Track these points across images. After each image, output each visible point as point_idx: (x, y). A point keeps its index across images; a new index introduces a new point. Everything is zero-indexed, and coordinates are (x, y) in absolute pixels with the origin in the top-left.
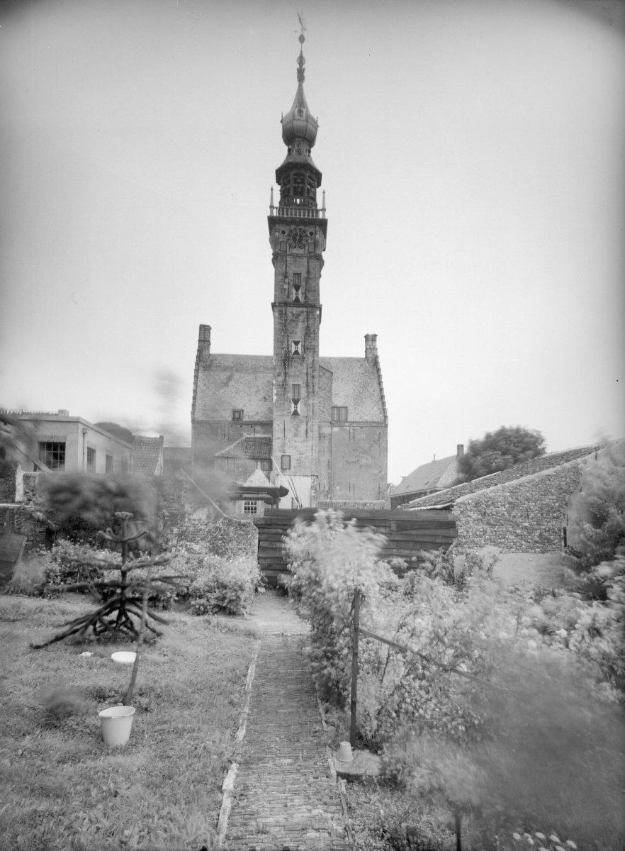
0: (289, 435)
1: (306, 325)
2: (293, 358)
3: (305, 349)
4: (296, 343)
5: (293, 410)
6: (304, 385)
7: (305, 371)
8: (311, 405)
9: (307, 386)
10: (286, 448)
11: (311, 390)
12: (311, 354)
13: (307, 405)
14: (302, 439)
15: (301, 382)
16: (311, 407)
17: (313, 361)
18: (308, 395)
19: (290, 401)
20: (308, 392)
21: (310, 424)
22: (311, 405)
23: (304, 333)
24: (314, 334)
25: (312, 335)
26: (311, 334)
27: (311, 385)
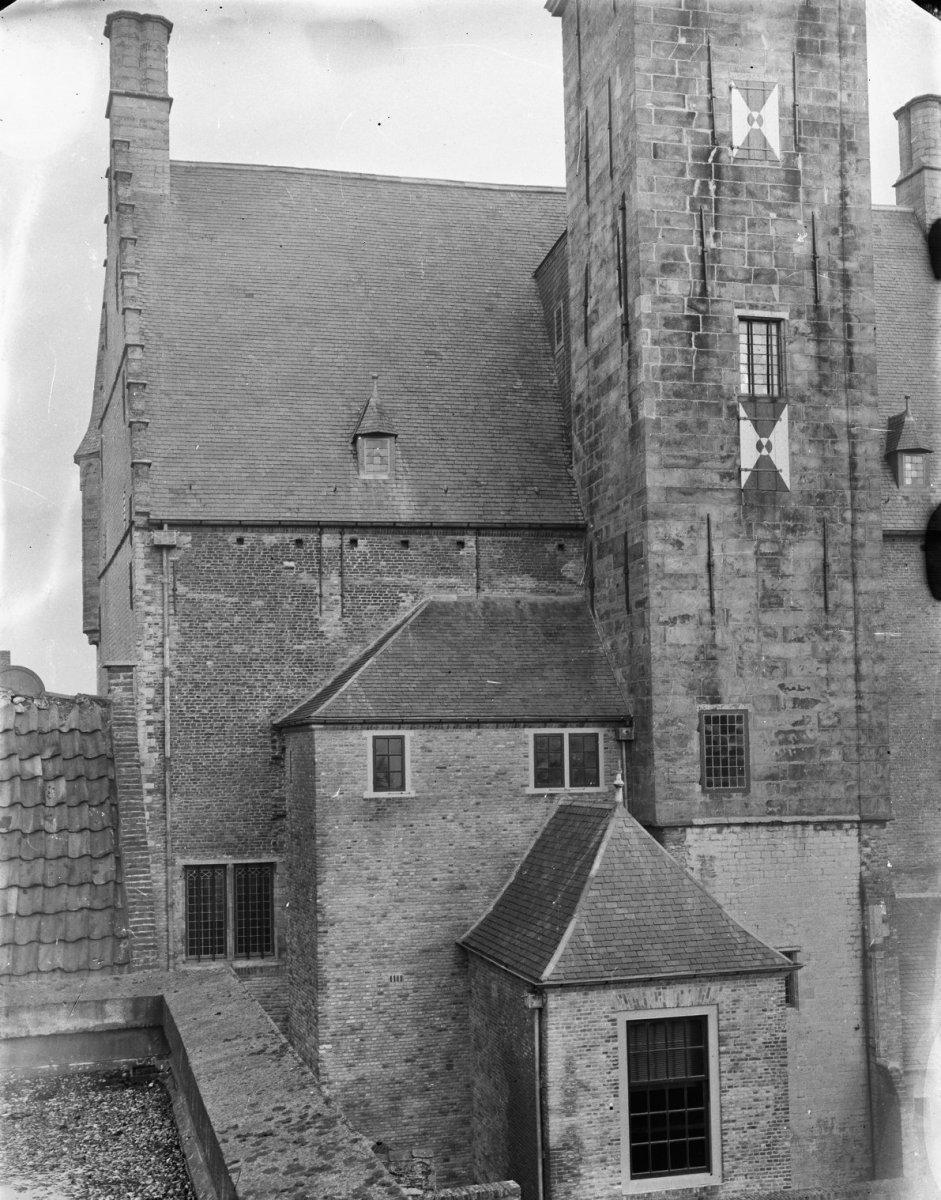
5: (748, 458)
6: (802, 324)
8: (842, 433)
9: (820, 330)
10: (724, 673)
11: (839, 349)
12: (830, 158)
13: (821, 434)
14: (804, 618)
16: (843, 447)
17: (844, 194)
19: (733, 412)
20: (821, 359)
21: (842, 533)
22: (842, 433)
24: (842, 50)
25: (832, 57)
26: (824, 48)
27: (835, 325)
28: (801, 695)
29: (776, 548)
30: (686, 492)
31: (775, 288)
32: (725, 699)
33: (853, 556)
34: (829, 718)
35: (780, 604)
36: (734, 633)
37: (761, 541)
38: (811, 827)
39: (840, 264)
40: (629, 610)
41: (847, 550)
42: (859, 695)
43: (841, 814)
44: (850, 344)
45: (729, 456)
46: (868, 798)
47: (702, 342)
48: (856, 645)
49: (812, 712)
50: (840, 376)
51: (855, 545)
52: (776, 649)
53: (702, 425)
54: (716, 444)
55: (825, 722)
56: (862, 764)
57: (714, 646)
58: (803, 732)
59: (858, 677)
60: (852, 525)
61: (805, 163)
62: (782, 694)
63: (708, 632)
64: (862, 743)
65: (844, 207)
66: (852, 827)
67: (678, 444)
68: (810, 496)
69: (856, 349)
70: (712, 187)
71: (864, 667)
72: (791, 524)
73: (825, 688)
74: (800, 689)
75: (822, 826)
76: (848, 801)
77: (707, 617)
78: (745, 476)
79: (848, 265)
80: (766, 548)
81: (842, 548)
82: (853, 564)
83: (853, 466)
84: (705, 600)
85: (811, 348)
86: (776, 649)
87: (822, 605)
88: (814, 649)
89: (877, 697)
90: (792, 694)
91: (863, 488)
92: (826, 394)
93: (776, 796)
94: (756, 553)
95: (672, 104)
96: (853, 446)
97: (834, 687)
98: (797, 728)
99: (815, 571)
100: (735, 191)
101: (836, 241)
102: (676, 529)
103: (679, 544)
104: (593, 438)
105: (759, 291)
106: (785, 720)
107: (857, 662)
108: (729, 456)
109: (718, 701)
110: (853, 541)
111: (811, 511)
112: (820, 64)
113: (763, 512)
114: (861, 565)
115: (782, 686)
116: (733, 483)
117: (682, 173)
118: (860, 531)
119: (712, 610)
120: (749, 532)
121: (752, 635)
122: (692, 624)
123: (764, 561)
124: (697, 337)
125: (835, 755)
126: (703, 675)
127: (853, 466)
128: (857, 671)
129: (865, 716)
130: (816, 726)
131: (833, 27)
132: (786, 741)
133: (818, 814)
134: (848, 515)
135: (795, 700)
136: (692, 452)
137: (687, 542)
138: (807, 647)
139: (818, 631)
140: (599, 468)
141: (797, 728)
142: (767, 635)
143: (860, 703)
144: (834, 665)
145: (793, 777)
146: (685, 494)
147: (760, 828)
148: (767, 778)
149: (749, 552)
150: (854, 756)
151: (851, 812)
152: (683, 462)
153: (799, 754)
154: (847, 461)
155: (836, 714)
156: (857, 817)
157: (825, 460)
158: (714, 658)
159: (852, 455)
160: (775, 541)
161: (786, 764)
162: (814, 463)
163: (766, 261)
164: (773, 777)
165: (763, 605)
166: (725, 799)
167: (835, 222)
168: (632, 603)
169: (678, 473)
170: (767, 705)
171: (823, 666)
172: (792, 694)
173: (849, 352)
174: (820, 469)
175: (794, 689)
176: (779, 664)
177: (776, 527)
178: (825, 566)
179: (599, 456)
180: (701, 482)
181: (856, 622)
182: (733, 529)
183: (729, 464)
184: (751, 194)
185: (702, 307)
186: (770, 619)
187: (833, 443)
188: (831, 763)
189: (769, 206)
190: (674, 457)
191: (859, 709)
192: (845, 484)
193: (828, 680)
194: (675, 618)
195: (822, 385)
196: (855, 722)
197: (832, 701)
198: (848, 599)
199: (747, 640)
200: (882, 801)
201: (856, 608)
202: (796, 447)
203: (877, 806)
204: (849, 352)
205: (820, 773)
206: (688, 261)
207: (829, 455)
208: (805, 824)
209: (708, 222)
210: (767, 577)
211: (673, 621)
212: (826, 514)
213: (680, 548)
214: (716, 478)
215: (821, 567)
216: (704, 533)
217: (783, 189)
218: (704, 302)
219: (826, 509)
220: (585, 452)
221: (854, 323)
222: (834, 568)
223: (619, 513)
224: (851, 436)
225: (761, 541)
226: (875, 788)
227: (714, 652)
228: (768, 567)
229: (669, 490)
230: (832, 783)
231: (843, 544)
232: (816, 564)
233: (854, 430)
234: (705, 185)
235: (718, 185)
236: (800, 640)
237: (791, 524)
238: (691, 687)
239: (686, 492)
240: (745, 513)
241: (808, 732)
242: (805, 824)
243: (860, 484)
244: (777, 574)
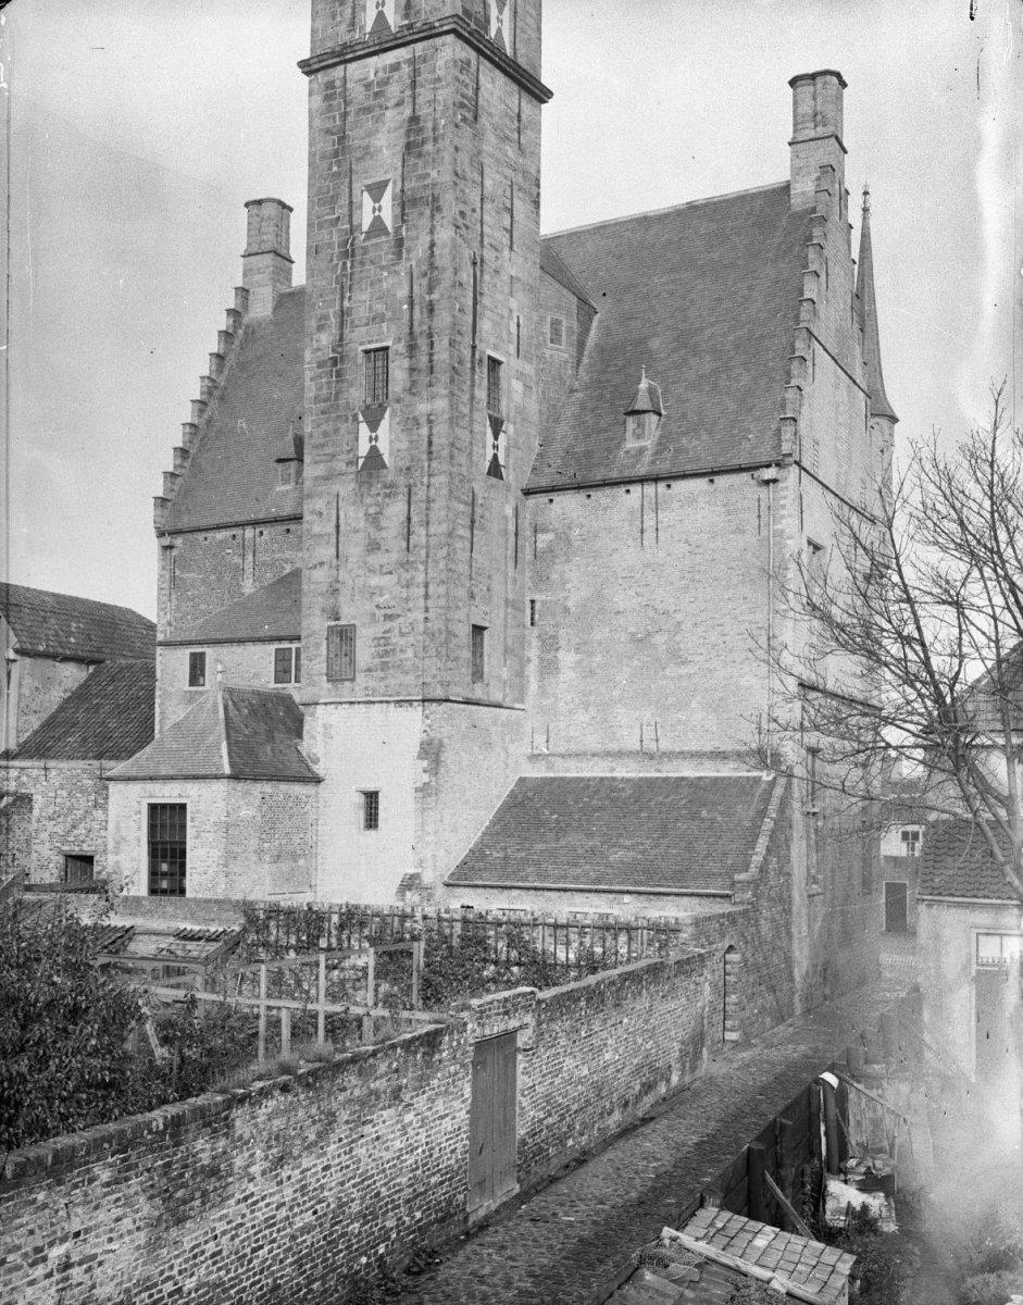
0: (354, 549)
1: (408, 112)
2: (365, 250)
3: (405, 204)
4: (376, 191)
5: (364, 449)
6: (401, 347)
7: (403, 293)
8: (423, 420)
9: (412, 348)
11: (424, 359)
13: (410, 423)
14: (394, 556)
15: (390, 336)
16: (424, 431)
18: (414, 383)
19: (355, 418)
20: (412, 370)
21: (420, 494)
22: (423, 420)
23: (400, 148)
25: (429, 147)
27: (423, 343)
28: (389, 612)
30: (326, 478)
31: (384, 325)
33: (427, 509)
35: (379, 549)
36: (350, 571)
37: (370, 506)
38: (393, 705)
39: (427, 298)
41: (424, 506)
43: (409, 695)
44: (431, 355)
47: (339, 374)
49: (395, 624)
50: (424, 379)
51: (429, 501)
52: (375, 581)
53: (336, 430)
59: (427, 596)
61: (407, 230)
62: (377, 612)
65: (432, 254)
69: (435, 357)
70: (349, 265)
71: (431, 589)
72: (388, 491)
74: (389, 608)
77: (335, 562)
78: (361, 461)
79: (433, 296)
82: (427, 515)
83: (430, 443)
84: (333, 551)
85: (406, 363)
86: (375, 581)
88: (399, 577)
90: (383, 612)
92: (414, 394)
95: (327, 214)
96: (431, 429)
100: (362, 263)
101: (425, 282)
105: (374, 328)
106: (378, 630)
109: (338, 619)
111: (402, 481)
112: (420, 155)
113: (371, 486)
114: (433, 516)
115: (377, 606)
116: (353, 469)
117: (331, 260)
118: (432, 491)
119: (338, 556)
124: (337, 371)
127: (430, 443)
129: (429, 625)
131: (430, 125)
135: (385, 616)
138: (394, 578)
139: (402, 565)
142: (370, 571)
148: (366, 671)
149: (361, 515)
154: (426, 439)
156: (420, 698)
157: (411, 442)
161: (377, 661)
163: (380, 307)
164: (369, 670)
165: (368, 551)
167: (424, 268)
169: (322, 466)
173: (431, 361)
174: (408, 449)
177: (379, 494)
184: (372, 262)
185: (340, 349)
186: (376, 560)
188: (406, 659)
189: (383, 268)
192: (424, 457)
193: (407, 600)
195: (412, 389)
198: (423, 541)
199: (357, 576)
201: (428, 547)
203: (435, 690)
204: (431, 361)
206: (333, 319)
207: (414, 438)
208: (387, 702)
209: (346, 289)
210: (371, 530)
212: (411, 481)
217: (393, 254)
218: (341, 346)
221: (435, 339)
222: (415, 519)
224: (430, 422)
225: (370, 506)
229: (317, 478)
230: (407, 673)
232: (403, 518)
233: (432, 418)
234: (344, 264)
235: (352, 262)
236: (390, 573)
237: (388, 491)
239: (326, 478)
243: (434, 455)
244: (380, 529)
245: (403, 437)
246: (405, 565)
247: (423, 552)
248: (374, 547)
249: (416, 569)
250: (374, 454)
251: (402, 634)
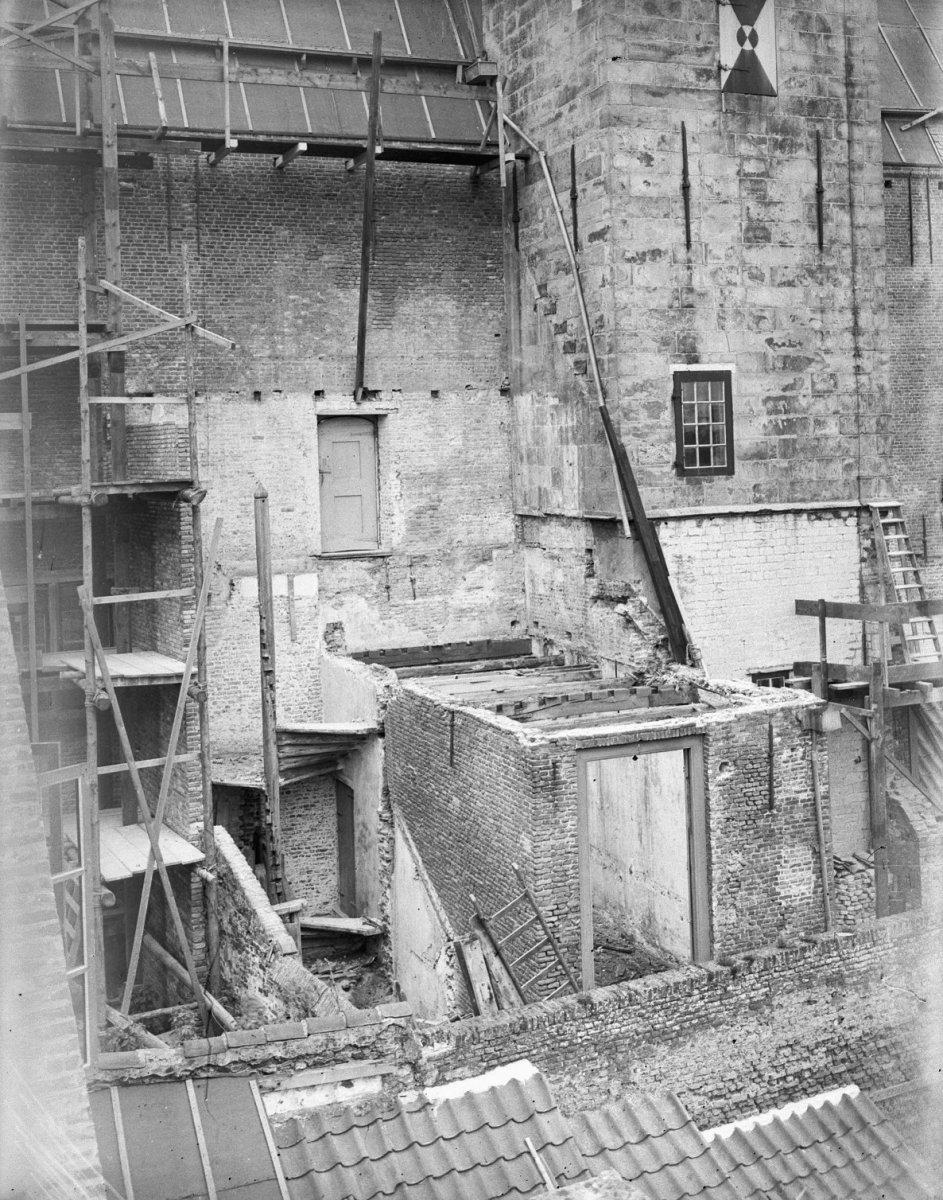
10: (703, 325)
14: (795, 258)
16: (839, 45)
21: (836, 153)
29: (762, 168)
32: (704, 358)
33: (850, 180)
34: (824, 380)
35: (767, 238)
36: (714, 274)
37: (749, 158)
38: (805, 516)
40: (577, 245)
42: (857, 354)
43: (837, 499)
45: (706, 49)
46: (869, 479)
48: (854, 291)
51: (852, 166)
52: (764, 296)
54: (691, 32)
55: (820, 386)
56: (862, 438)
57: (691, 290)
58: (795, 398)
60: (849, 142)
62: (770, 351)
63: (683, 273)
64: (861, 411)
66: (851, 516)
67: (645, 29)
68: (801, 103)
71: (865, 318)
72: (779, 137)
73: (819, 344)
74: (791, 345)
75: (817, 514)
76: (846, 483)
77: (682, 254)
78: (725, 76)
80: (751, 167)
81: (837, 170)
87: (816, 241)
88: (807, 295)
89: (877, 354)
90: (783, 351)
91: (860, 95)
93: (762, 479)
94: (738, 173)
97: (829, 343)
98: (788, 394)
99: (806, 198)
102: (645, 139)
103: (648, 159)
104: (516, 33)
107: (855, 311)
108: (706, 49)
109: (696, 360)
110: (851, 161)
111: (801, 121)
113: (747, 122)
116: (712, 84)
119: (688, 245)
120: (732, 146)
121: (736, 278)
122: (664, 262)
123: (748, 184)
125: (832, 428)
126: (677, 328)
128: (856, 323)
129: (864, 379)
130: (810, 391)
132: (776, 411)
133: (812, 500)
134: (844, 128)
136: (662, 41)
137: (657, 156)
138: (798, 293)
139: (811, 273)
140: (529, 69)
141: (788, 394)
142: (753, 277)
143: (859, 362)
144: (830, 316)
145: (784, 456)
146: (654, 94)
147: (746, 519)
149: (731, 170)
150: (853, 429)
151: (850, 498)
152: (650, 53)
153: (790, 426)
155: (832, 376)
156: (856, 503)
157: (817, 59)
158: (691, 306)
159: (848, 55)
160: (760, 159)
161: (775, 439)
162: (804, 62)
166: (704, 484)
168: (583, 235)
169: (647, 66)
170: (754, 365)
171: (818, 316)
172: (783, 351)
174: (812, 70)
175: (784, 344)
176: (766, 314)
177: (762, 141)
178: (820, 192)
179: (529, 54)
180: (673, 80)
181: (854, 262)
182: (715, 140)
183: (706, 59)
186: (757, 257)
187: (827, 38)
188: (827, 438)
190: (641, 46)
191: (858, 370)
192: (840, 90)
194: (644, 254)
196: (854, 386)
197: (828, 359)
198: (845, 234)
200: (883, 482)
201: (853, 245)
202: (783, 42)
205: (815, 451)
207: (821, 53)
208: (798, 512)
210: (751, 204)
211: (640, 258)
212: (819, 127)
213: (649, 165)
214: (692, 77)
215: (813, 193)
216: (678, 146)
219: (819, 121)
220: (506, 52)
222: (828, 195)
223: (562, 122)
224: (848, 31)
226: (876, 467)
227: (691, 298)
228: (753, 191)
229: (634, 88)
230: (829, 461)
231: (838, 165)
232: (809, 189)
233: (850, 24)
236: (790, 284)
237: (779, 137)
238: (665, 342)
240: (725, 123)
241: (800, 398)
242: (798, 512)
243: (857, 90)
244: (765, 202)
245: (800, 45)
246: (816, 272)
247: (847, 253)
248: (759, 233)
249: (836, 283)
250: (748, 66)
251: (818, 395)
